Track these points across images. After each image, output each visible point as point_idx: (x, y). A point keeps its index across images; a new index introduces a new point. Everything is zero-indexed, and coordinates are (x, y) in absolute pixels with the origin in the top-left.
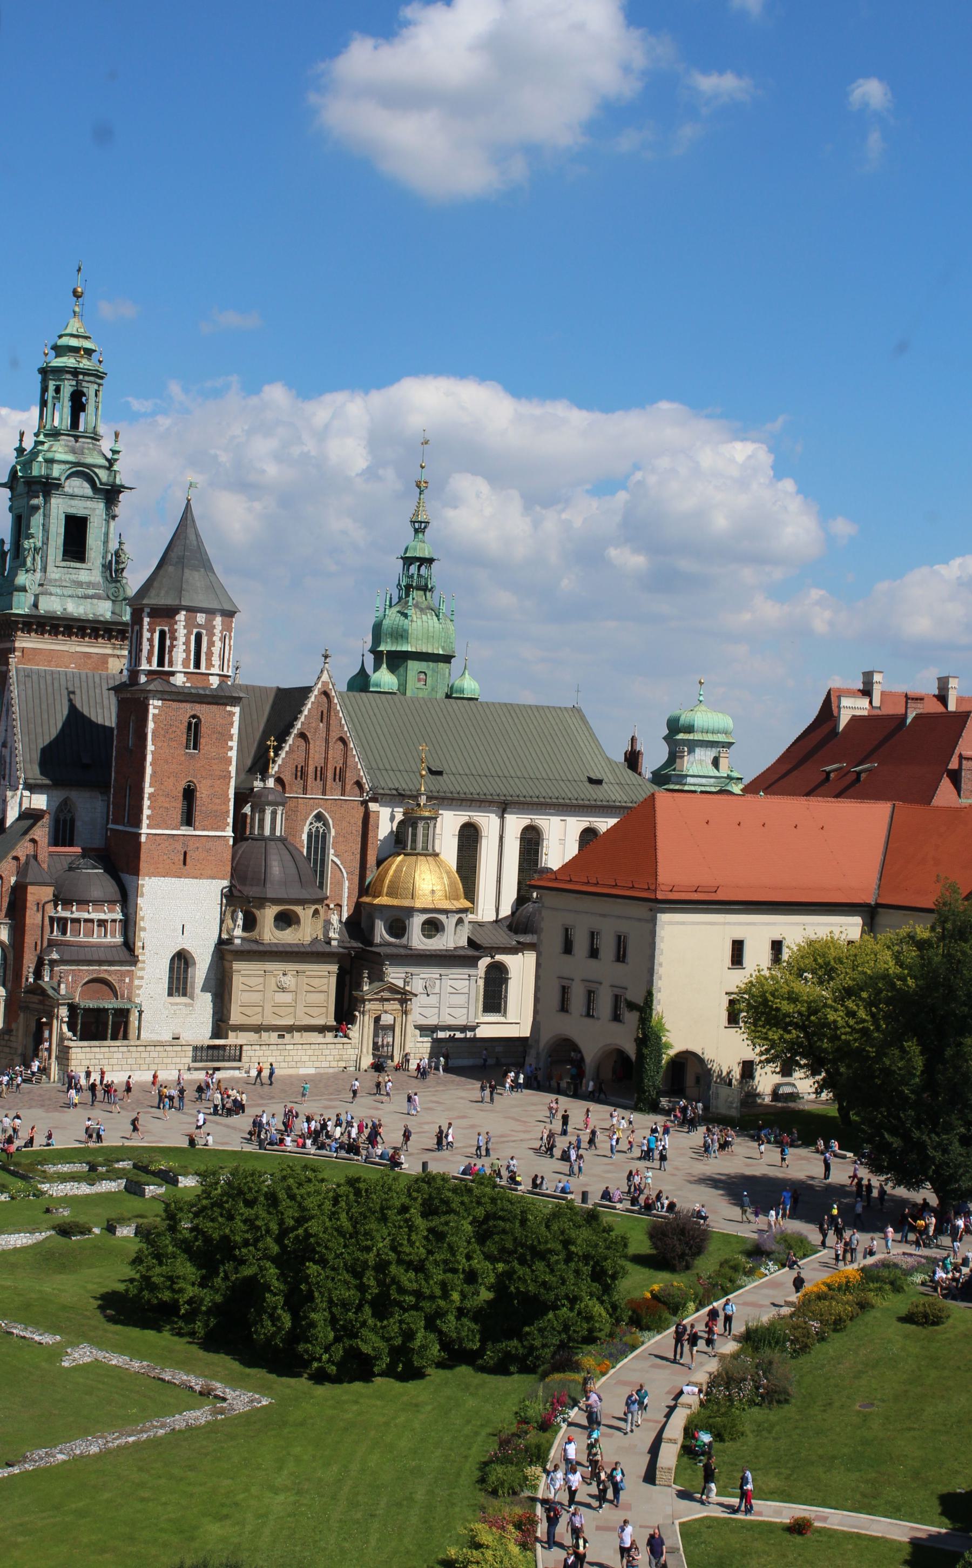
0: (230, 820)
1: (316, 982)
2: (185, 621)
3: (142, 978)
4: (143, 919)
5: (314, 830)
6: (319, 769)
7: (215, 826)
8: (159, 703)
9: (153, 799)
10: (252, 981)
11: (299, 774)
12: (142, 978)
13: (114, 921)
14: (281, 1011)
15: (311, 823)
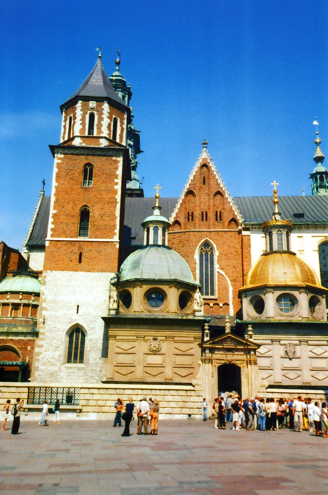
0: (117, 231)
1: (184, 347)
2: (82, 106)
3: (42, 346)
4: (45, 301)
5: (204, 253)
6: (204, 213)
7: (105, 235)
8: (62, 156)
9: (56, 217)
10: (126, 346)
11: (190, 217)
12: (42, 346)
13: (25, 305)
14: (154, 371)
15: (202, 249)
